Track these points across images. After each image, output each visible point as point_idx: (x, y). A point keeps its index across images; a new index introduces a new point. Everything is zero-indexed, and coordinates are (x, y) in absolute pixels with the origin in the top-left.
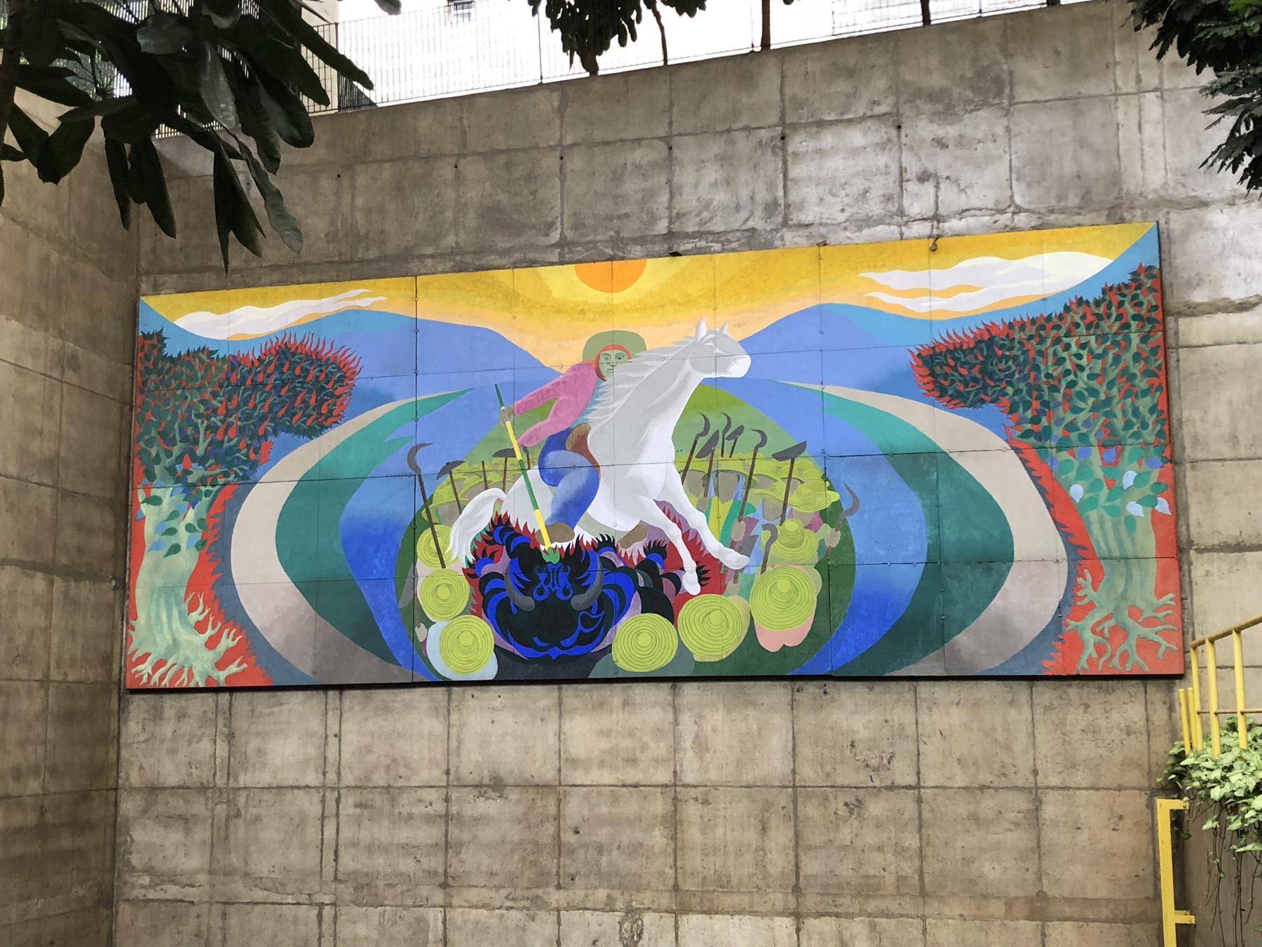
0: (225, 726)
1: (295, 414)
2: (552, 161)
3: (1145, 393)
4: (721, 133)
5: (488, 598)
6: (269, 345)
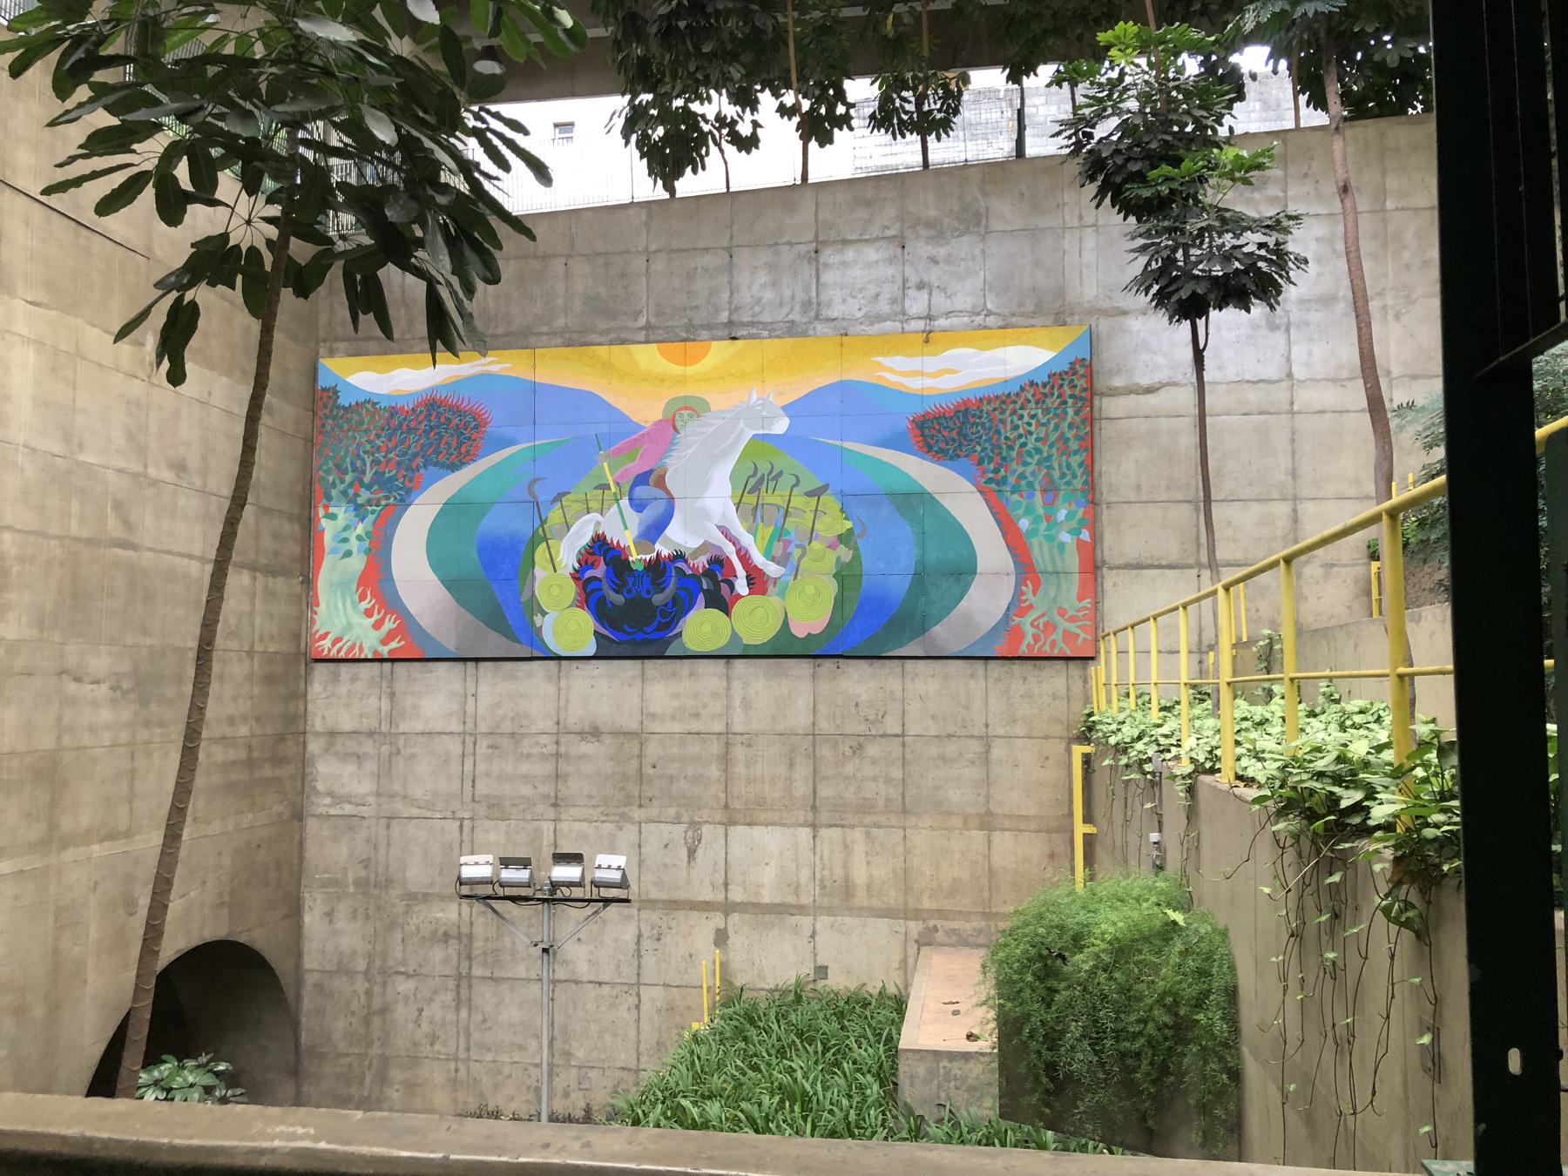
2: (639, 263)
3: (1076, 452)
5: (590, 596)
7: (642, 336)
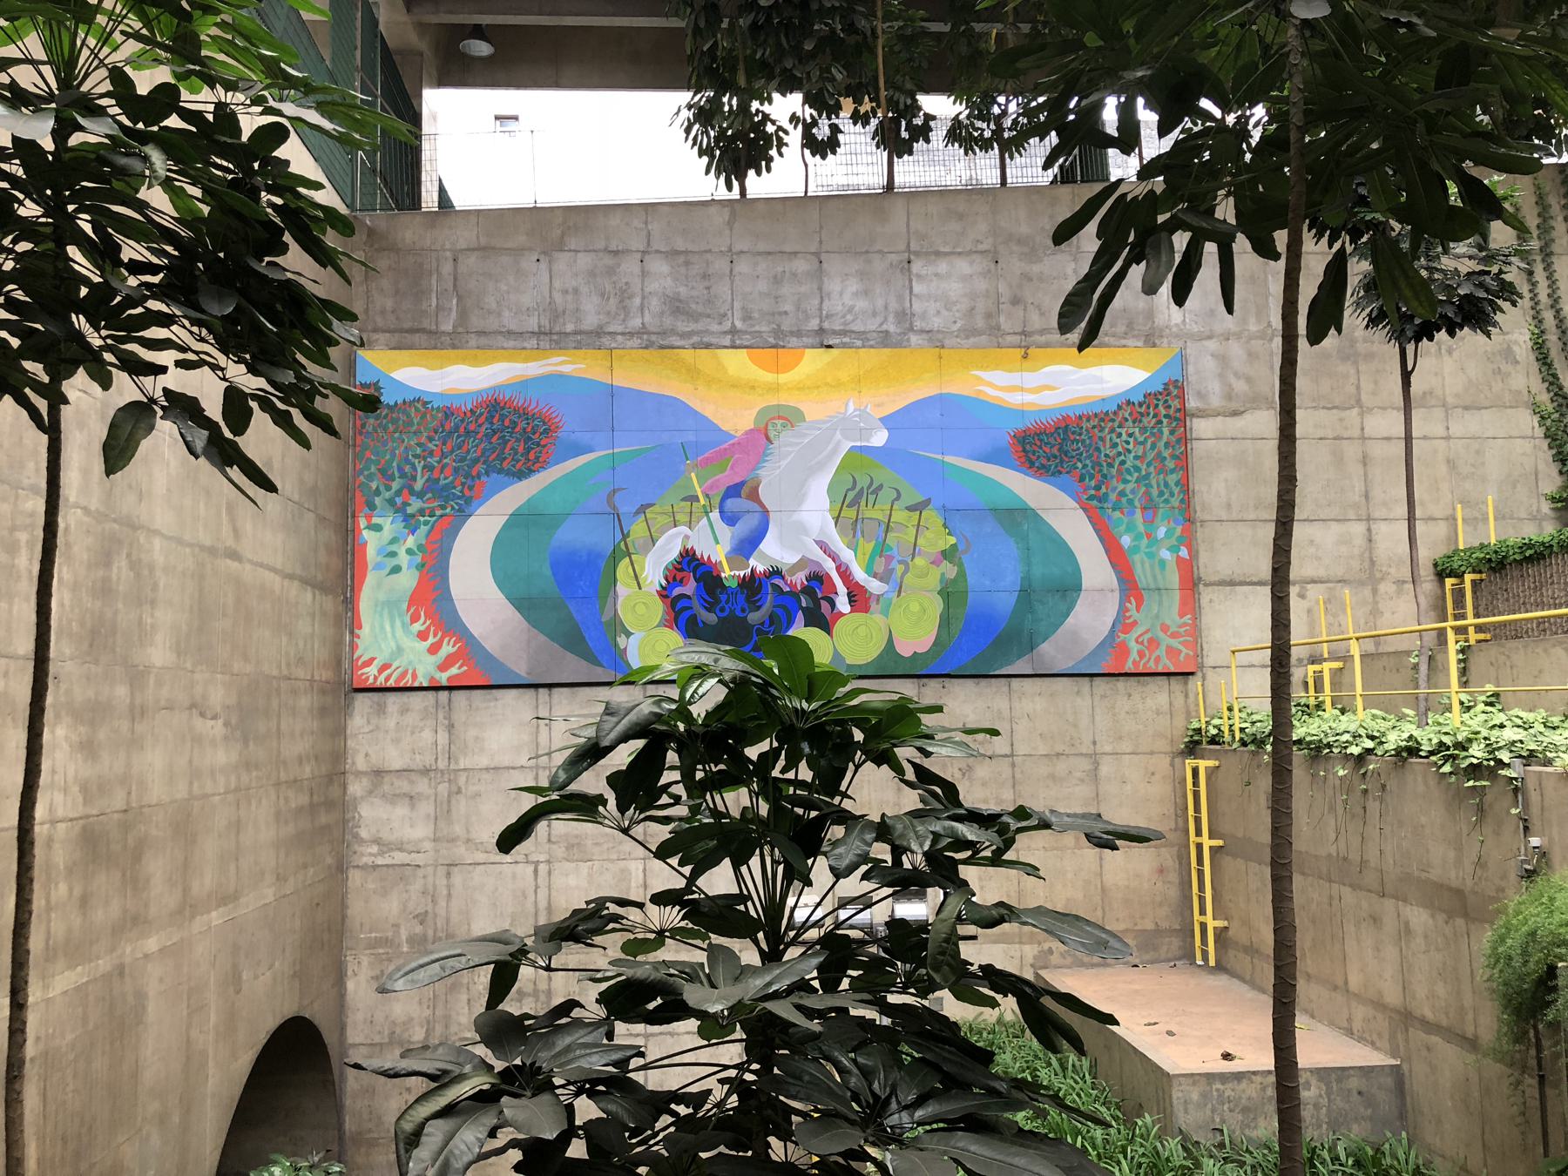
2: (721, 265)
3: (1172, 471)
7: (727, 341)
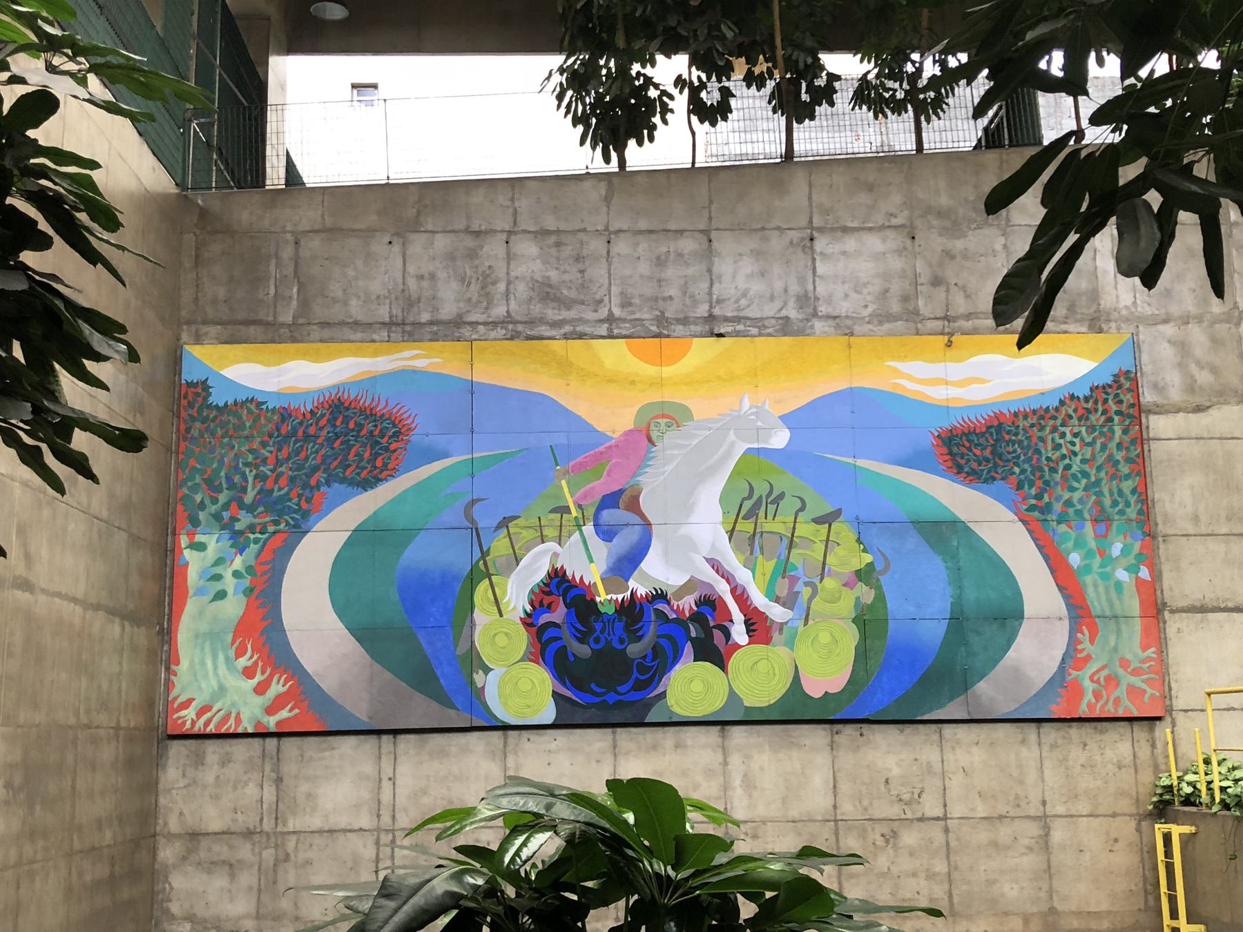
0: (272, 771)
1: (349, 466)
2: (596, 245)
3: (1127, 477)
4: (756, 230)
5: (545, 645)
6: (321, 400)
7: (603, 329)
